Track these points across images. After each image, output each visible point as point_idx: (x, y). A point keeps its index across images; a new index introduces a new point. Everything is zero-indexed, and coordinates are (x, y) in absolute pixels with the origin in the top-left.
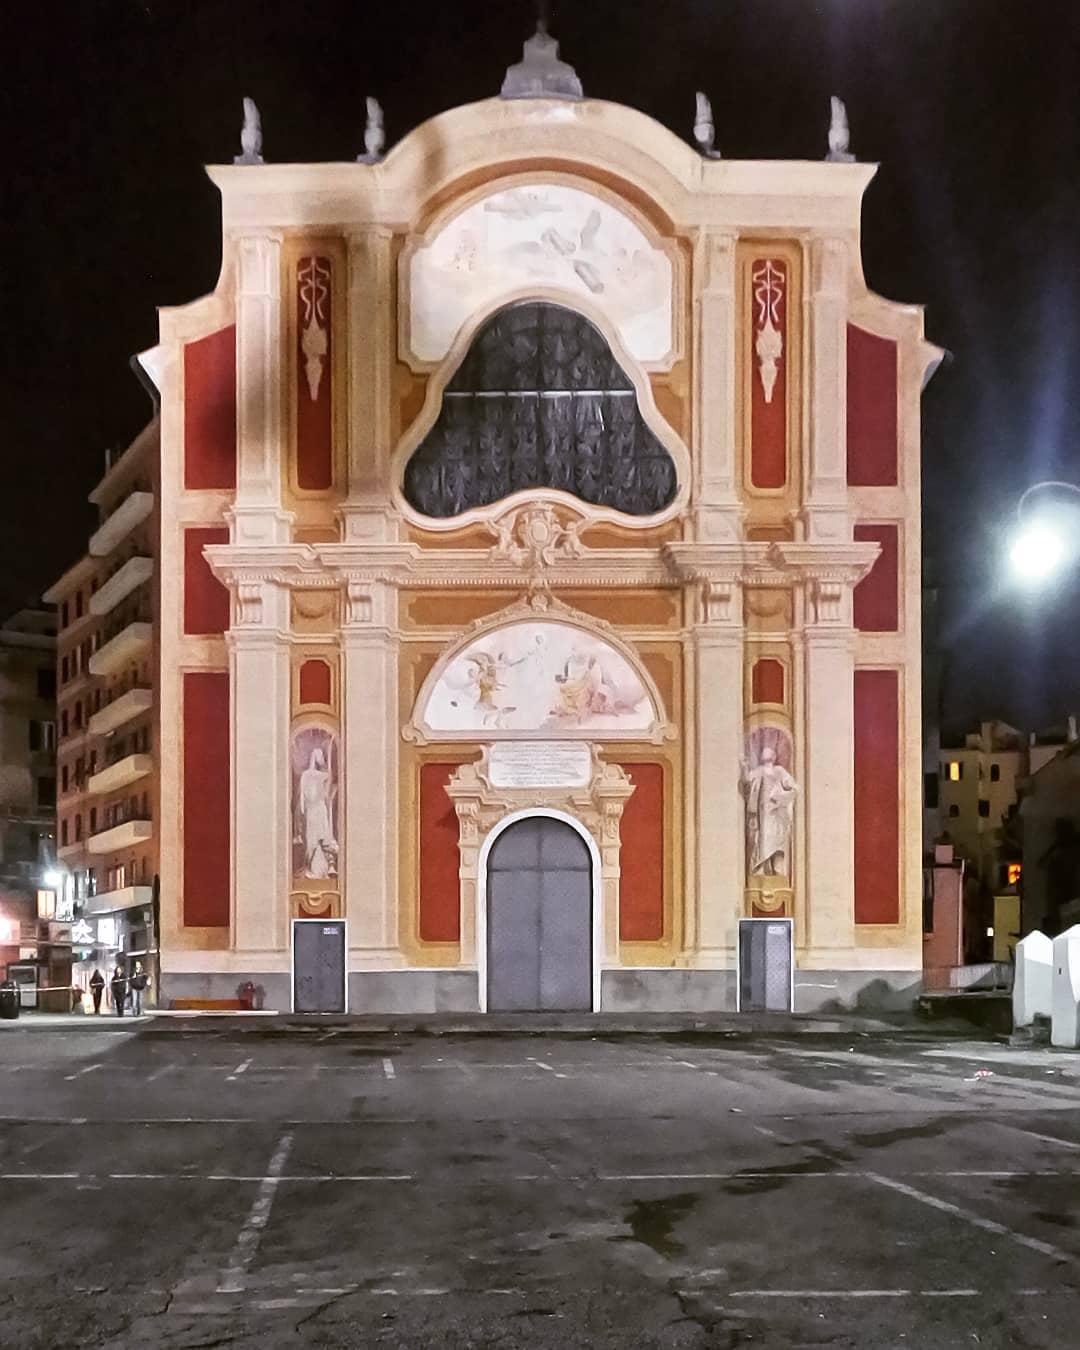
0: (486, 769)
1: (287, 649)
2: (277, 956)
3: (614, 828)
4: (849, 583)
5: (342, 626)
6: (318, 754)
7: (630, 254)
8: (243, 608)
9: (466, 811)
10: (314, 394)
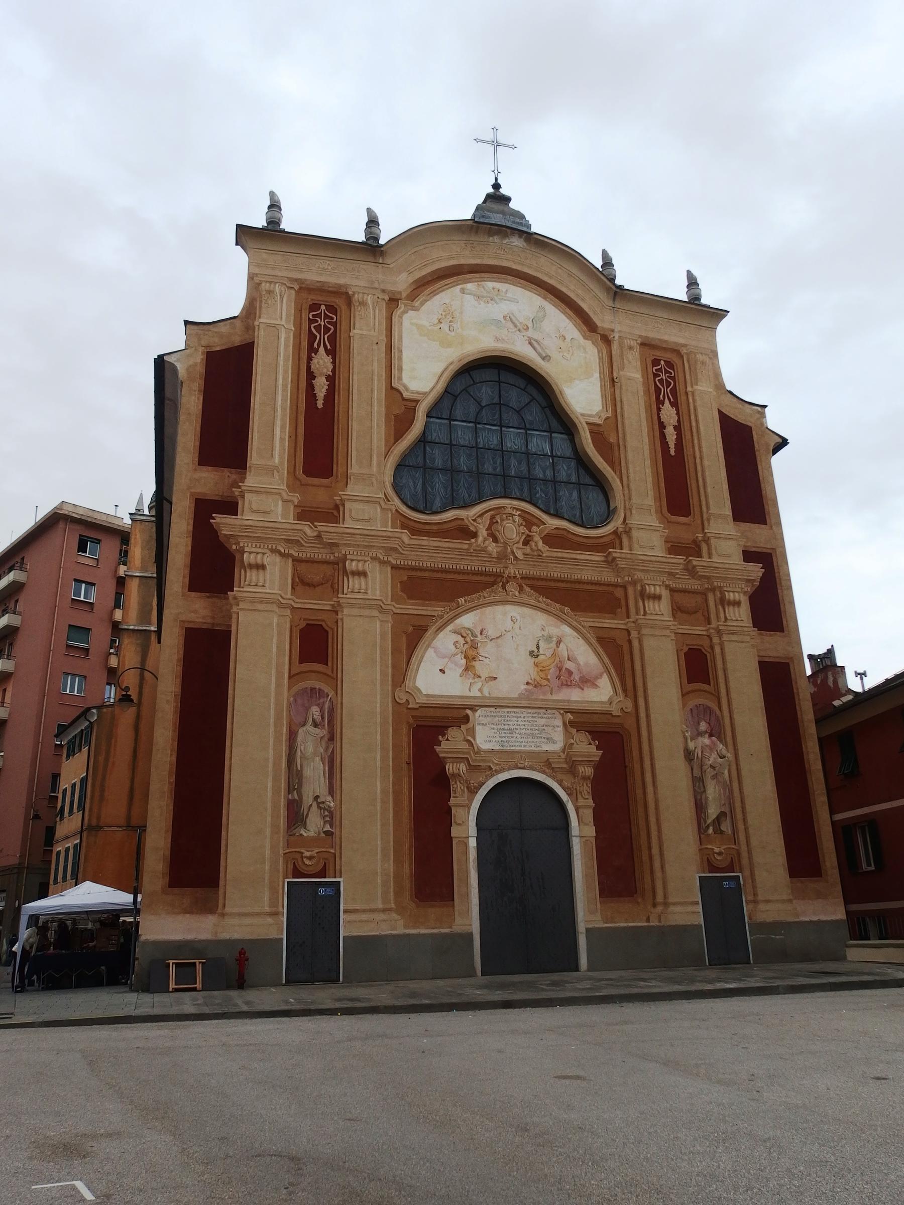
0: (472, 731)
1: (288, 612)
2: (269, 920)
3: (586, 788)
4: (745, 593)
5: (340, 596)
6: (315, 711)
7: (568, 338)
8: (248, 574)
9: (456, 771)
10: (320, 404)
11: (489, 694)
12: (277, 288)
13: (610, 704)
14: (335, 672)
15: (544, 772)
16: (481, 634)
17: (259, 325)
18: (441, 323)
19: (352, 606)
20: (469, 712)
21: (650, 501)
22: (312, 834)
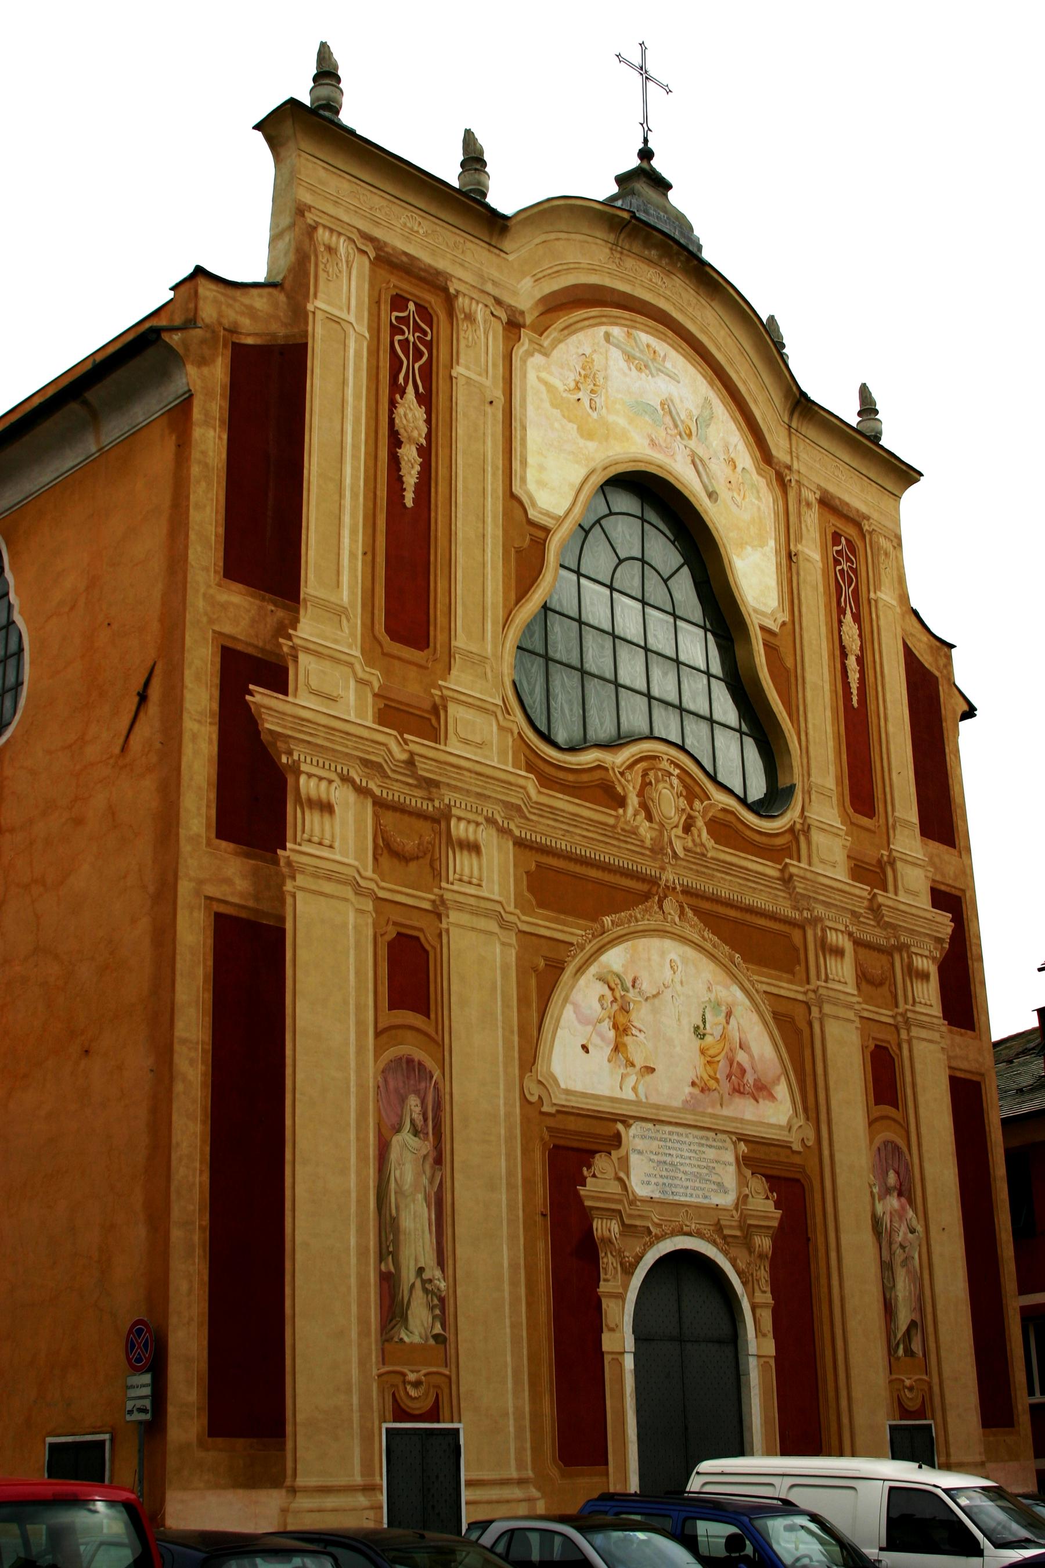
0: (625, 1163)
1: (369, 906)
2: (362, 1500)
3: (763, 1275)
4: (934, 959)
7: (739, 469)
9: (606, 1233)
10: (409, 502)
11: (646, 1098)
12: (343, 247)
13: (790, 1131)
14: (440, 1032)
15: (714, 1243)
16: (633, 986)
17: (314, 313)
18: (579, 389)
19: (460, 907)
20: (620, 1127)
21: (830, 783)
22: (417, 1339)
